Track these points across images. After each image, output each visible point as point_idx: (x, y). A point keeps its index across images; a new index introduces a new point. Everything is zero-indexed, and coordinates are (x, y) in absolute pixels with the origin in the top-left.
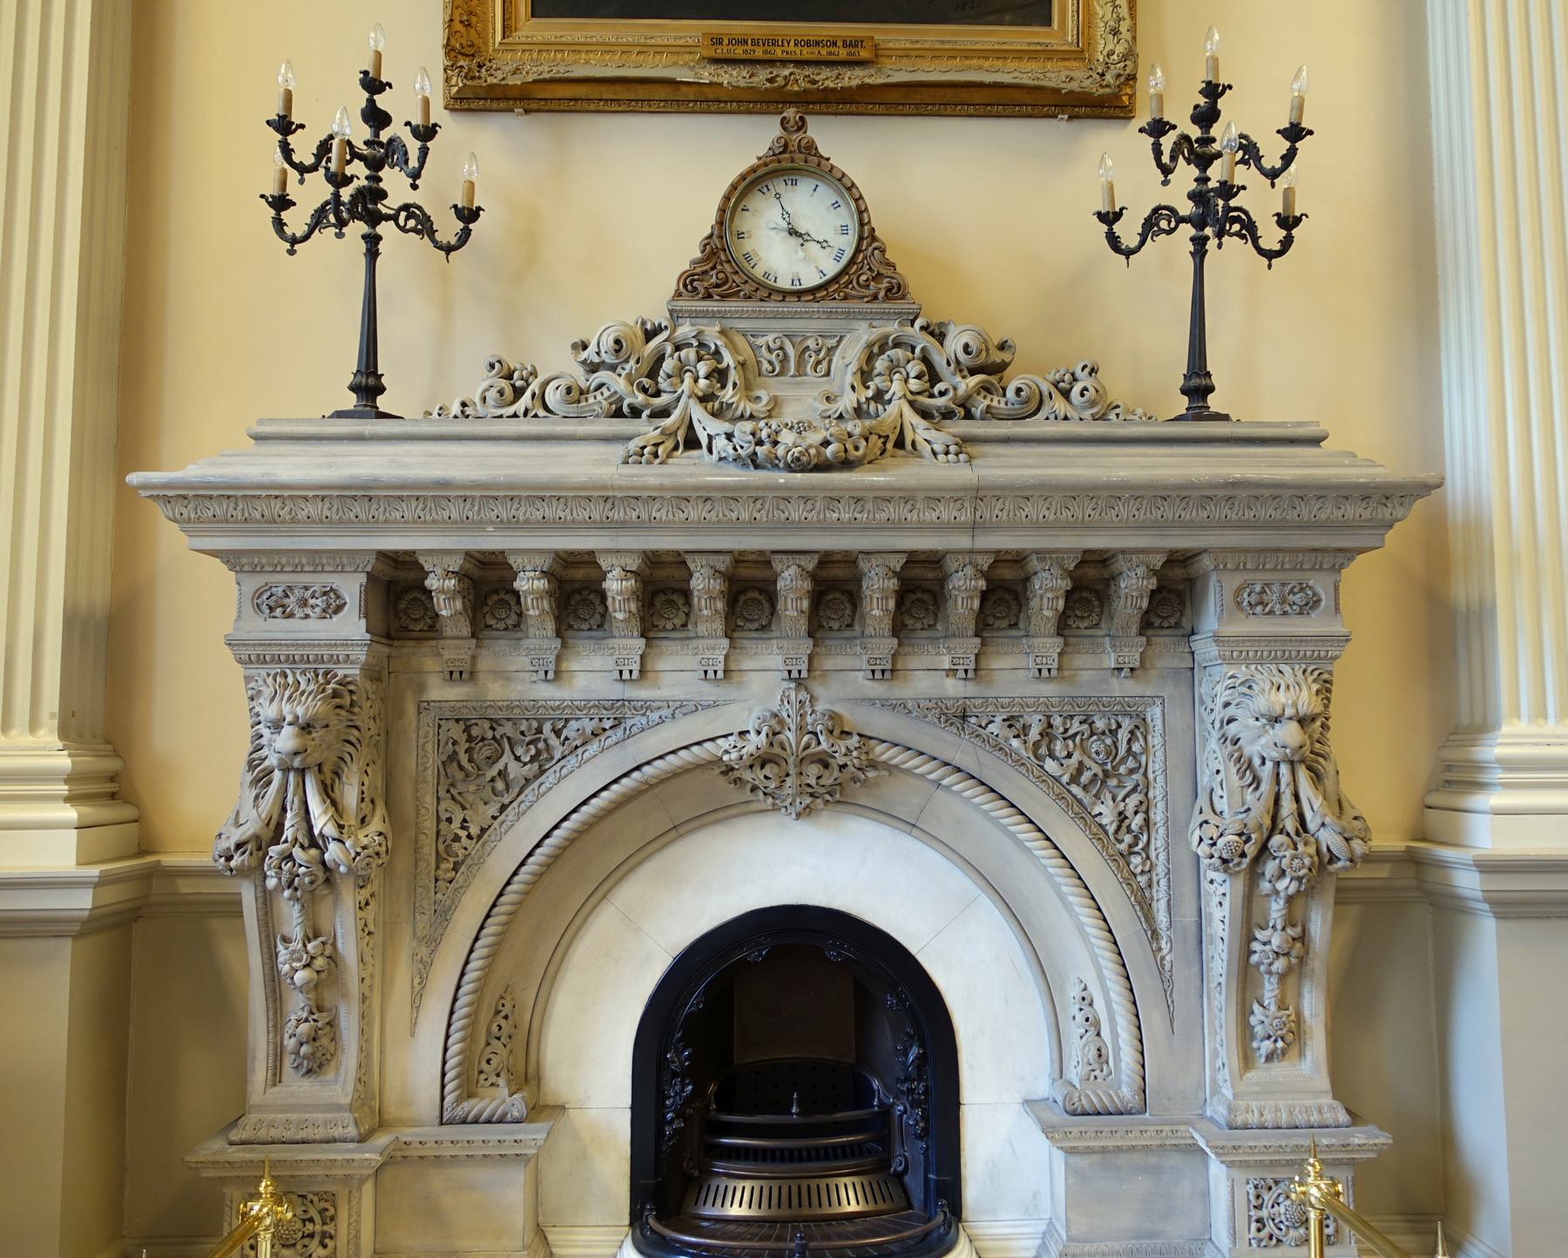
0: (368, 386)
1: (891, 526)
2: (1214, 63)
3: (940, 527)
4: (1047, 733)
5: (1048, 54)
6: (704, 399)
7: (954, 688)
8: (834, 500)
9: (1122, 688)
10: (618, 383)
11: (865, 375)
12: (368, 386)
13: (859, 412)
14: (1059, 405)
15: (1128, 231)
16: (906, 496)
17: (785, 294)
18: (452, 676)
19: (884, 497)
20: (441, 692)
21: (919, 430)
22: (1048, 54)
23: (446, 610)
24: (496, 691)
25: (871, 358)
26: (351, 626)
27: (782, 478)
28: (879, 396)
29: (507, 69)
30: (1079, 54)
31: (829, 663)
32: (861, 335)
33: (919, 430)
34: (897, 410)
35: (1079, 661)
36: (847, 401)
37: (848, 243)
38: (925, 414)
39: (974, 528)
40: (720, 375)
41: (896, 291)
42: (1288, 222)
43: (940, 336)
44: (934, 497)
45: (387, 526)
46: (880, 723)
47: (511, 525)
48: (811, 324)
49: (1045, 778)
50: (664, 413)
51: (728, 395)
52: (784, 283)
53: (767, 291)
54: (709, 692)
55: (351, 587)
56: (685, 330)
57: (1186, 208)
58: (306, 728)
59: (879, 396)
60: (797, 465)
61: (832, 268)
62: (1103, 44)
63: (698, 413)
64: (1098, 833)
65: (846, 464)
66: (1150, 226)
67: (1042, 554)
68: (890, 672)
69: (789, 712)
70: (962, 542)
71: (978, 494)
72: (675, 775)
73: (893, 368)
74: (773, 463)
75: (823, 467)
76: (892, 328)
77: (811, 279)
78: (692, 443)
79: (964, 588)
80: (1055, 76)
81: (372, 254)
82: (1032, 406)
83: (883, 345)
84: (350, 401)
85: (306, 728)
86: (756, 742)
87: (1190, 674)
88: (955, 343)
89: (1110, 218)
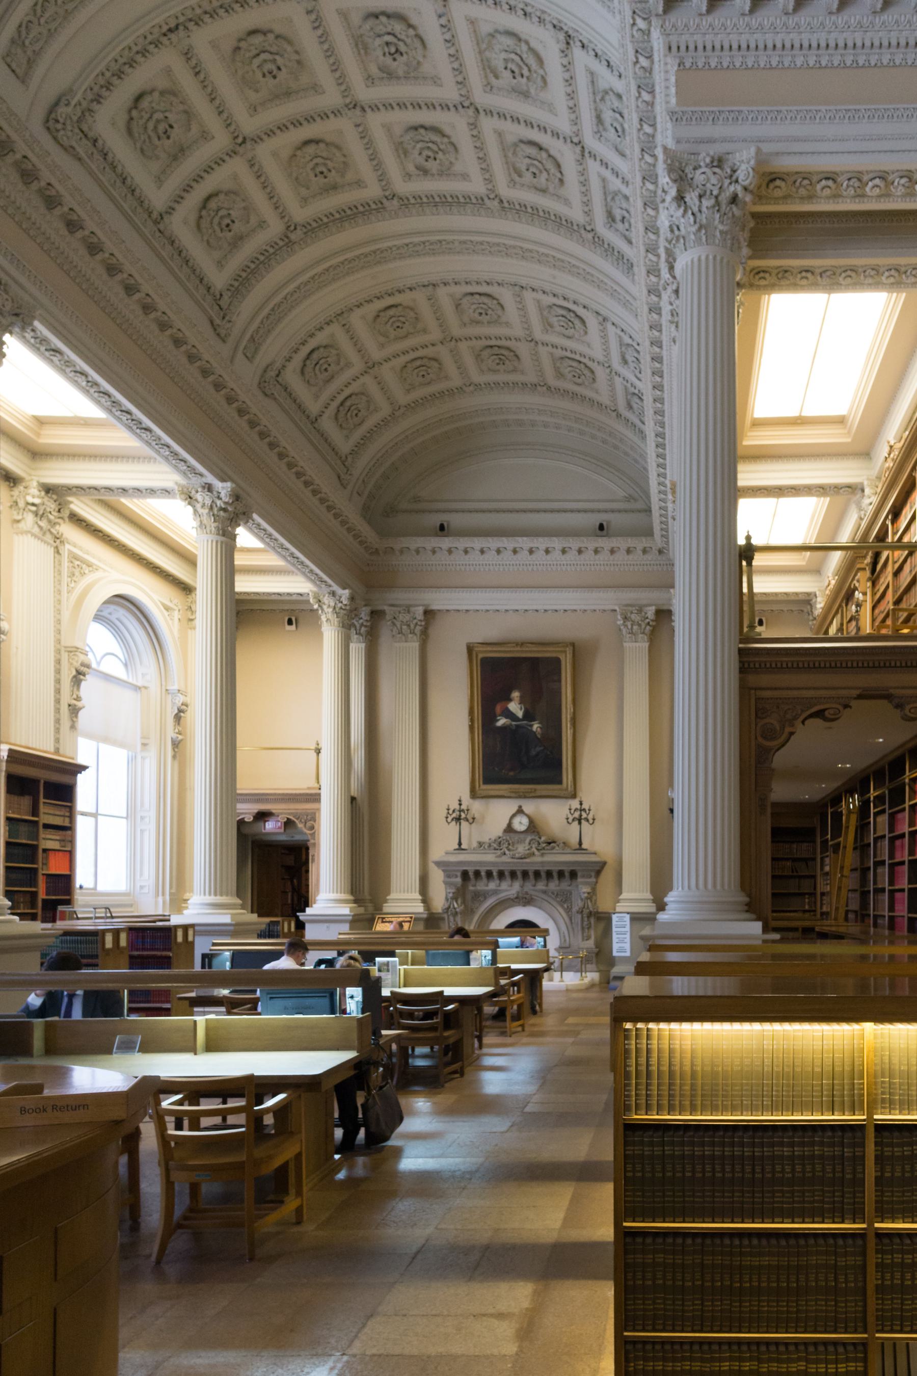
48: (522, 836)
53: (516, 832)
88: (543, 839)
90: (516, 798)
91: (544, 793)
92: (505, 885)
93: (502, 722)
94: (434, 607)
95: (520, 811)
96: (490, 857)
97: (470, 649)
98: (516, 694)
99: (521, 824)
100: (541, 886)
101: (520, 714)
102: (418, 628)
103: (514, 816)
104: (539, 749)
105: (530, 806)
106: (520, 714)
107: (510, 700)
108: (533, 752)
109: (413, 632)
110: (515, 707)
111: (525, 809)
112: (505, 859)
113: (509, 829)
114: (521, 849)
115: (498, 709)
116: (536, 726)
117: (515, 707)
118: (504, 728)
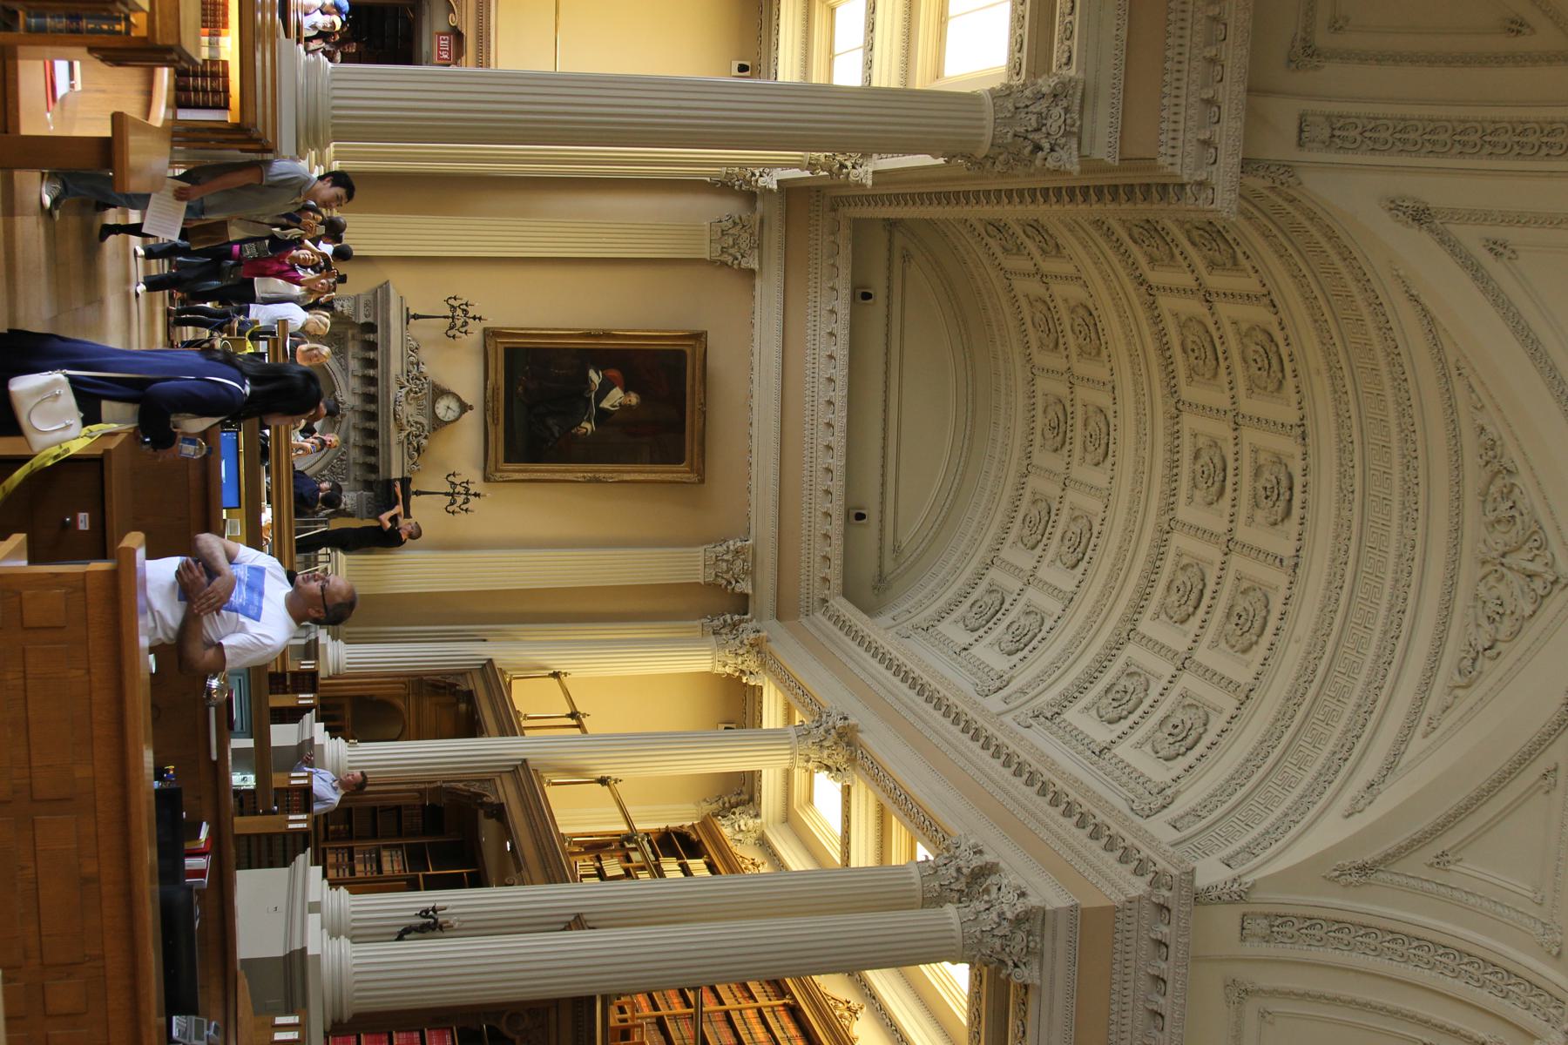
0: (416, 317)
1: (383, 429)
2: (485, 496)
3: (383, 438)
4: (342, 460)
5: (496, 462)
6: (411, 390)
7: (352, 441)
8: (388, 417)
9: (352, 477)
10: (414, 372)
11: (416, 423)
12: (416, 317)
13: (408, 422)
14: (411, 462)
15: (451, 478)
16: (389, 431)
17: (434, 406)
18: (353, 336)
19: (388, 427)
20: (350, 333)
21: (404, 434)
22: (496, 462)
23: (366, 337)
24: (350, 344)
25: (420, 424)
26: (362, 320)
27: (392, 408)
28: (412, 426)
29: (491, 342)
30: (497, 470)
31: (357, 414)
32: (425, 422)
33: (404, 434)
34: (409, 429)
35: (358, 467)
36: (410, 419)
37: (446, 419)
38: (408, 434)
39: (383, 445)
40: (416, 393)
41: (435, 429)
42: (453, 512)
43: (426, 437)
44: (389, 437)
45: (382, 327)
46: (344, 425)
47: (382, 352)
48: (427, 411)
49: (332, 460)
50: (408, 381)
51: (412, 395)
52: (437, 405)
53: (434, 402)
54: (350, 389)
55: (370, 320)
56: (426, 386)
57: (456, 491)
58: (342, 312)
59: (412, 426)
60: (394, 410)
61: (440, 416)
62: (499, 474)
63: (407, 389)
64: (321, 470)
65: (395, 419)
66: (452, 483)
67: (378, 459)
68: (354, 427)
69: (346, 406)
70: (380, 442)
71: (389, 445)
72: (333, 382)
73: (418, 429)
74: (395, 405)
75: (395, 415)
76: (426, 428)
77: (437, 411)
78: (401, 388)
79: (372, 443)
80: (491, 463)
81: (445, 317)
82: (411, 457)
83: (423, 426)
84: (412, 313)
85: (342, 312)
86: (340, 399)
87: (355, 491)
88: (424, 442)
89: (454, 475)
90: (486, 402)
91: (491, 438)
92: (355, 383)
93: (595, 377)
94: (758, 282)
95: (464, 408)
96: (396, 367)
97: (699, 337)
98: (633, 399)
99: (445, 409)
100: (354, 437)
101: (605, 404)
102: (729, 260)
103: (459, 399)
104: (556, 430)
105: (472, 420)
106: (605, 404)
107: (625, 391)
108: (550, 422)
109: (723, 250)
110: (616, 398)
111: (468, 415)
112: (394, 387)
113: (439, 392)
114: (408, 411)
115: (614, 373)
116: (588, 427)
117: (615, 397)
118: (587, 380)
